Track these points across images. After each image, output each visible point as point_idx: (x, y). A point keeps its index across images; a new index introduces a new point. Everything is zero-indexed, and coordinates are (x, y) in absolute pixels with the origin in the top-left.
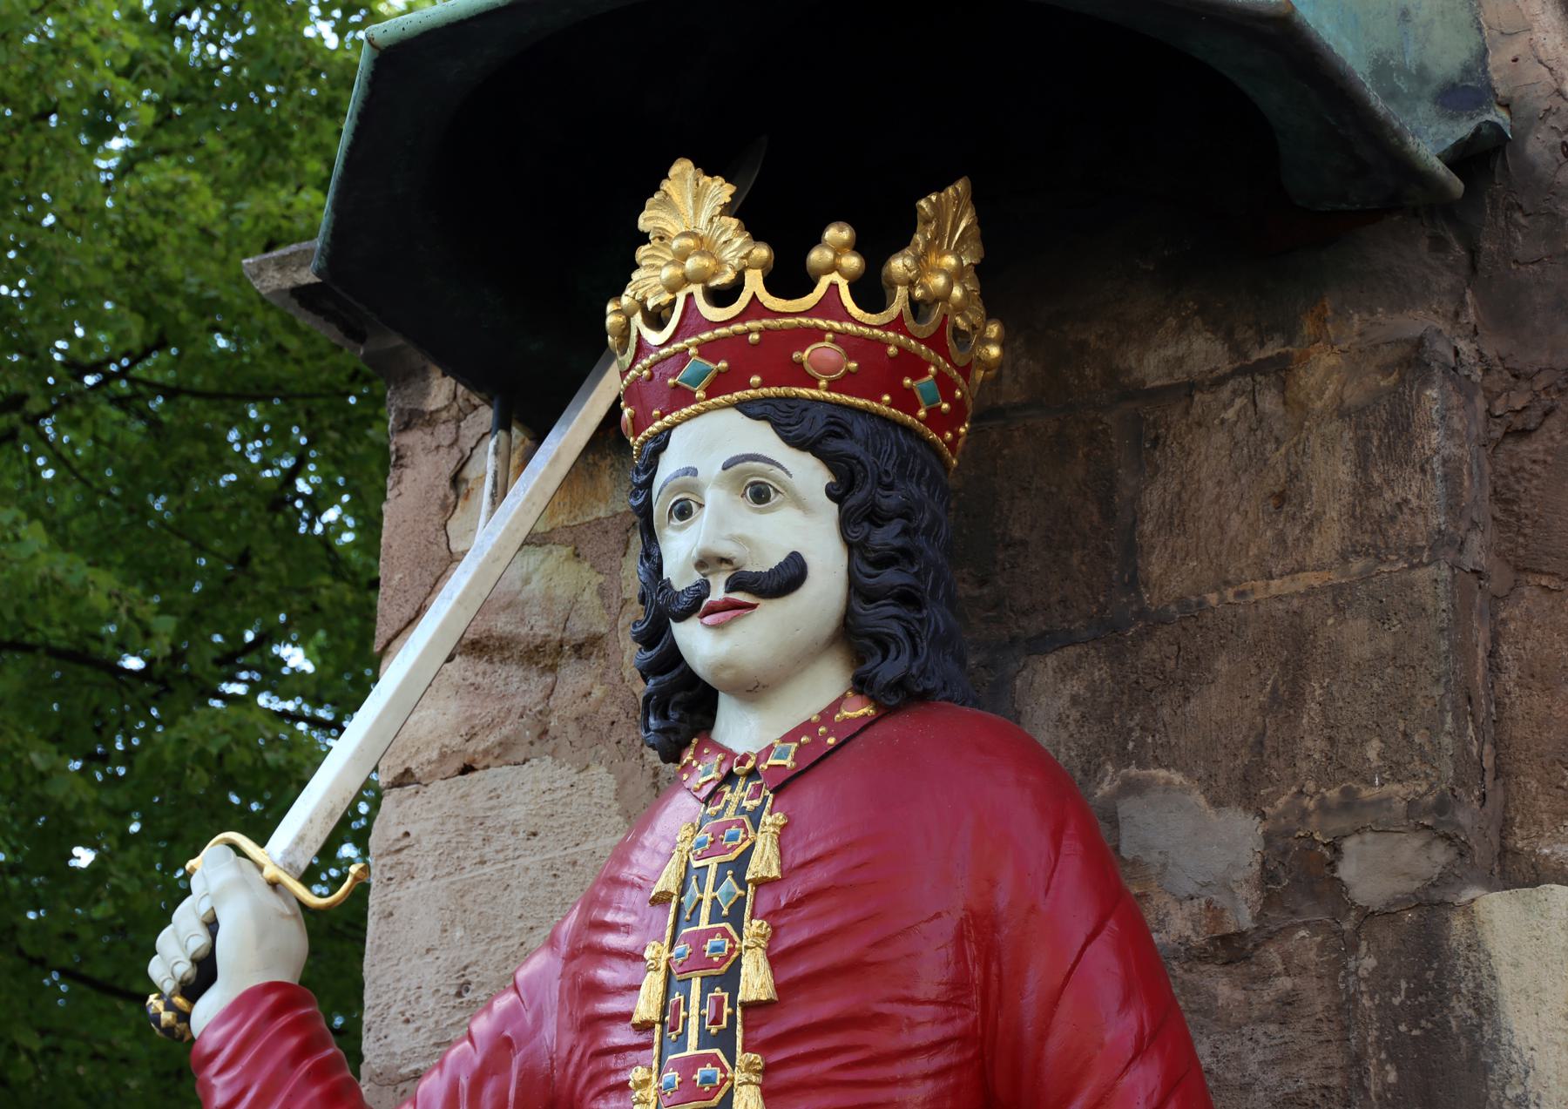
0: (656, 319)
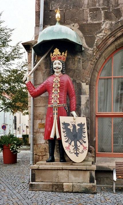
0: (55, 55)
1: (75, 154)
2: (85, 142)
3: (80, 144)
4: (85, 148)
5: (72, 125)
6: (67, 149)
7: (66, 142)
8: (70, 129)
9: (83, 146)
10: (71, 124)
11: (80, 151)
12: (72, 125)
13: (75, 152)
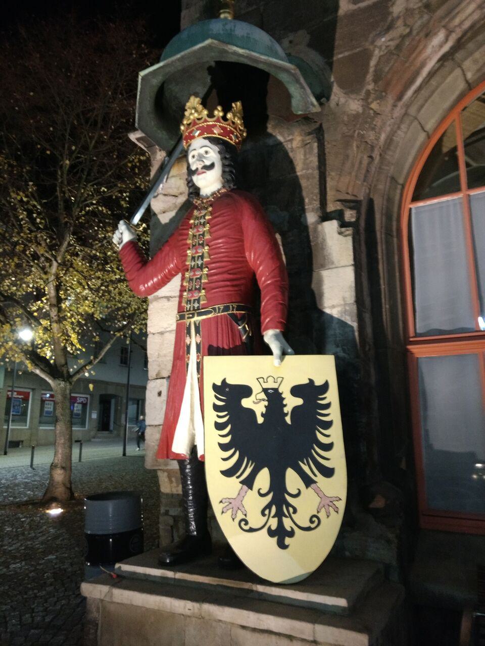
1: (271, 533)
2: (328, 472)
3: (302, 486)
4: (328, 503)
5: (265, 391)
6: (229, 512)
7: (228, 473)
8: (251, 413)
9: (318, 492)
10: (256, 389)
11: (302, 519)
12: (265, 391)
13: (274, 523)
